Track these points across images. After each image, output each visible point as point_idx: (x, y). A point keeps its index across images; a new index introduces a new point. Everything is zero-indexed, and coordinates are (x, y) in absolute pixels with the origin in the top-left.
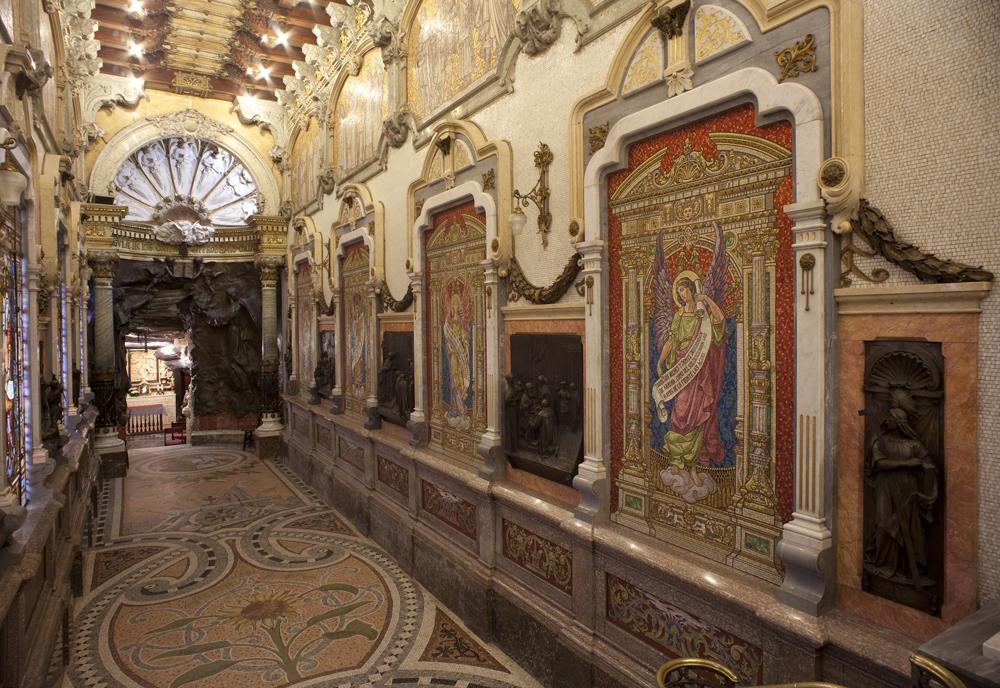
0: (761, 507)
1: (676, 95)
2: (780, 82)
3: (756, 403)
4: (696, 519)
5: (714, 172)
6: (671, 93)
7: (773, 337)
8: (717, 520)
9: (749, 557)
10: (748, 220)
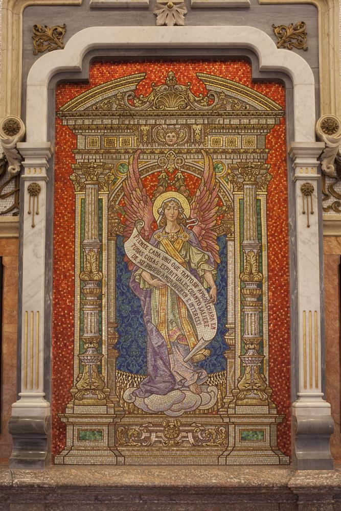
0: (254, 401)
1: (165, 25)
2: (278, 48)
3: (248, 311)
4: (180, 431)
5: (203, 107)
6: (160, 20)
7: (264, 254)
8: (206, 425)
9: (247, 449)
10: (240, 153)
